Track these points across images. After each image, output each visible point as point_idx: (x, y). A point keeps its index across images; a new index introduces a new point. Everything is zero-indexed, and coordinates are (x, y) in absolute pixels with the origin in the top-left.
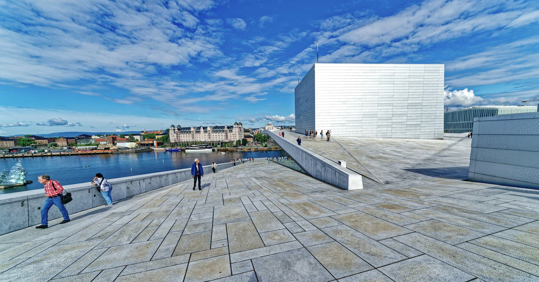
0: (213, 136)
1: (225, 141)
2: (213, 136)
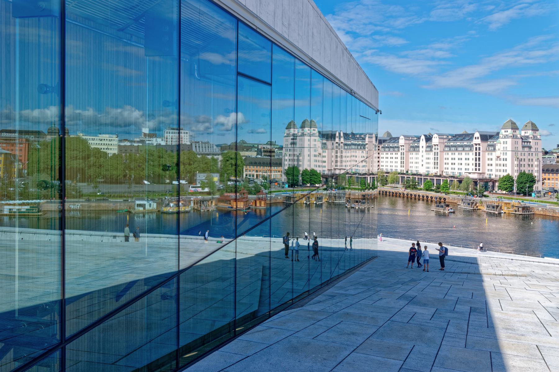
0: (446, 161)
2: (446, 161)
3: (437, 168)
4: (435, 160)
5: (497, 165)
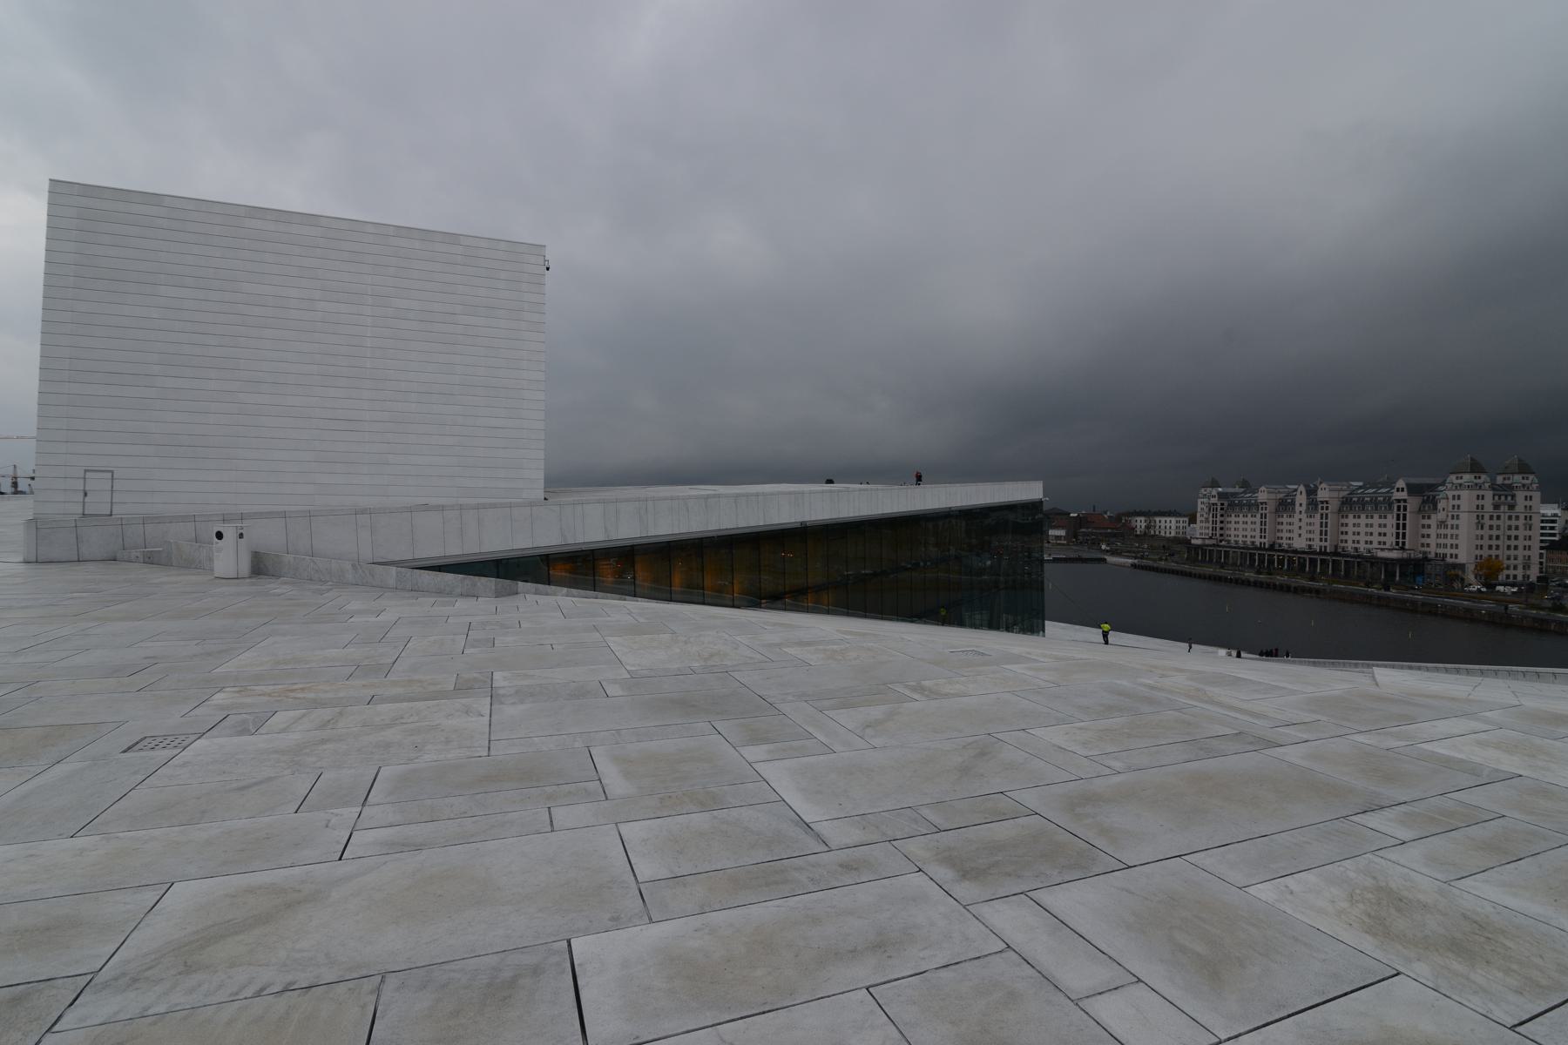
1: (1381, 554)
3: (1326, 540)
4: (1321, 526)
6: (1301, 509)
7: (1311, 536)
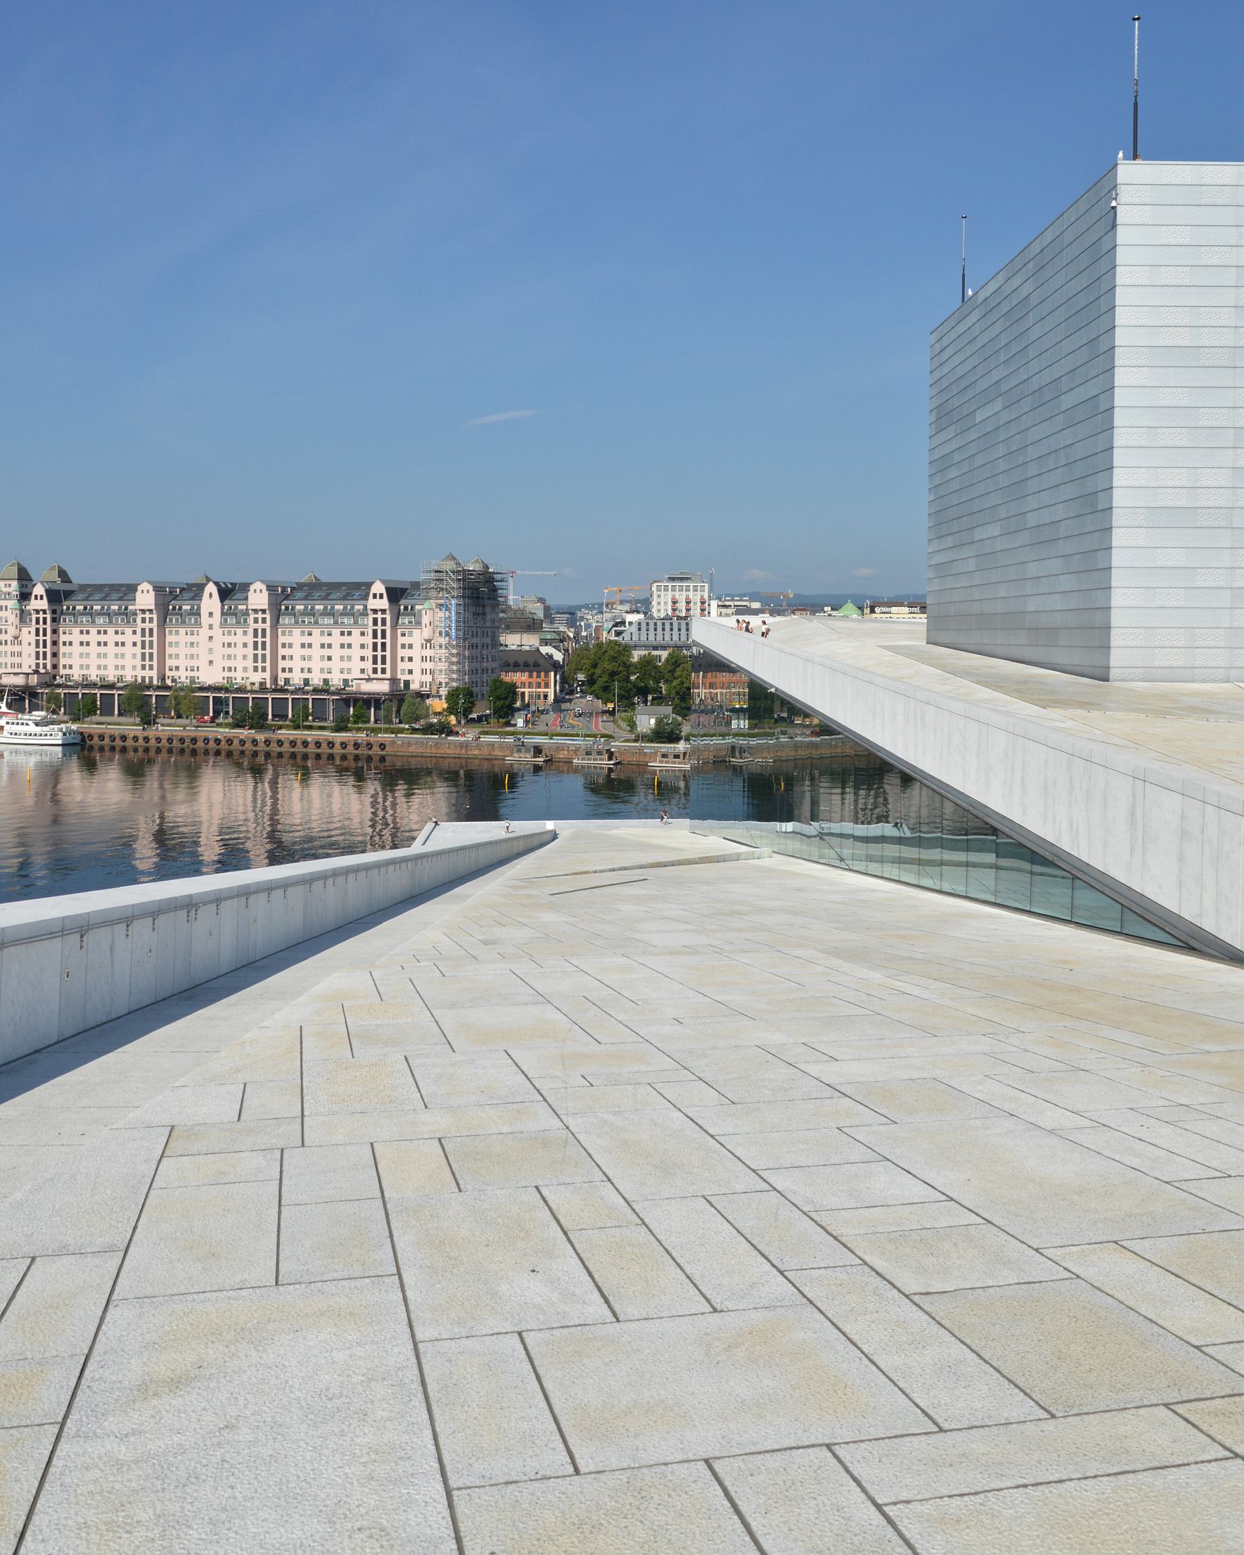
1: (367, 687)
5: (423, 659)
6: (211, 621)
7: (232, 664)
